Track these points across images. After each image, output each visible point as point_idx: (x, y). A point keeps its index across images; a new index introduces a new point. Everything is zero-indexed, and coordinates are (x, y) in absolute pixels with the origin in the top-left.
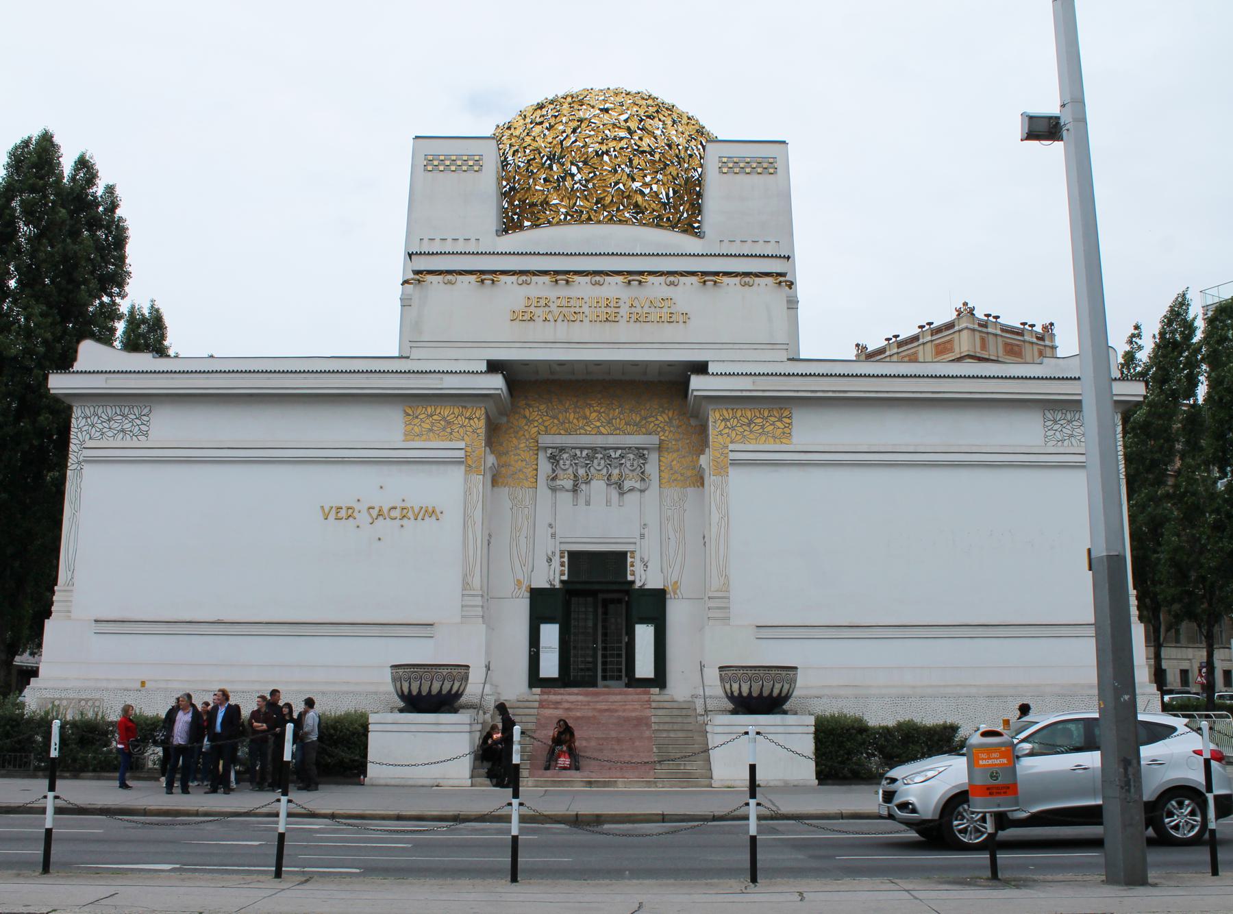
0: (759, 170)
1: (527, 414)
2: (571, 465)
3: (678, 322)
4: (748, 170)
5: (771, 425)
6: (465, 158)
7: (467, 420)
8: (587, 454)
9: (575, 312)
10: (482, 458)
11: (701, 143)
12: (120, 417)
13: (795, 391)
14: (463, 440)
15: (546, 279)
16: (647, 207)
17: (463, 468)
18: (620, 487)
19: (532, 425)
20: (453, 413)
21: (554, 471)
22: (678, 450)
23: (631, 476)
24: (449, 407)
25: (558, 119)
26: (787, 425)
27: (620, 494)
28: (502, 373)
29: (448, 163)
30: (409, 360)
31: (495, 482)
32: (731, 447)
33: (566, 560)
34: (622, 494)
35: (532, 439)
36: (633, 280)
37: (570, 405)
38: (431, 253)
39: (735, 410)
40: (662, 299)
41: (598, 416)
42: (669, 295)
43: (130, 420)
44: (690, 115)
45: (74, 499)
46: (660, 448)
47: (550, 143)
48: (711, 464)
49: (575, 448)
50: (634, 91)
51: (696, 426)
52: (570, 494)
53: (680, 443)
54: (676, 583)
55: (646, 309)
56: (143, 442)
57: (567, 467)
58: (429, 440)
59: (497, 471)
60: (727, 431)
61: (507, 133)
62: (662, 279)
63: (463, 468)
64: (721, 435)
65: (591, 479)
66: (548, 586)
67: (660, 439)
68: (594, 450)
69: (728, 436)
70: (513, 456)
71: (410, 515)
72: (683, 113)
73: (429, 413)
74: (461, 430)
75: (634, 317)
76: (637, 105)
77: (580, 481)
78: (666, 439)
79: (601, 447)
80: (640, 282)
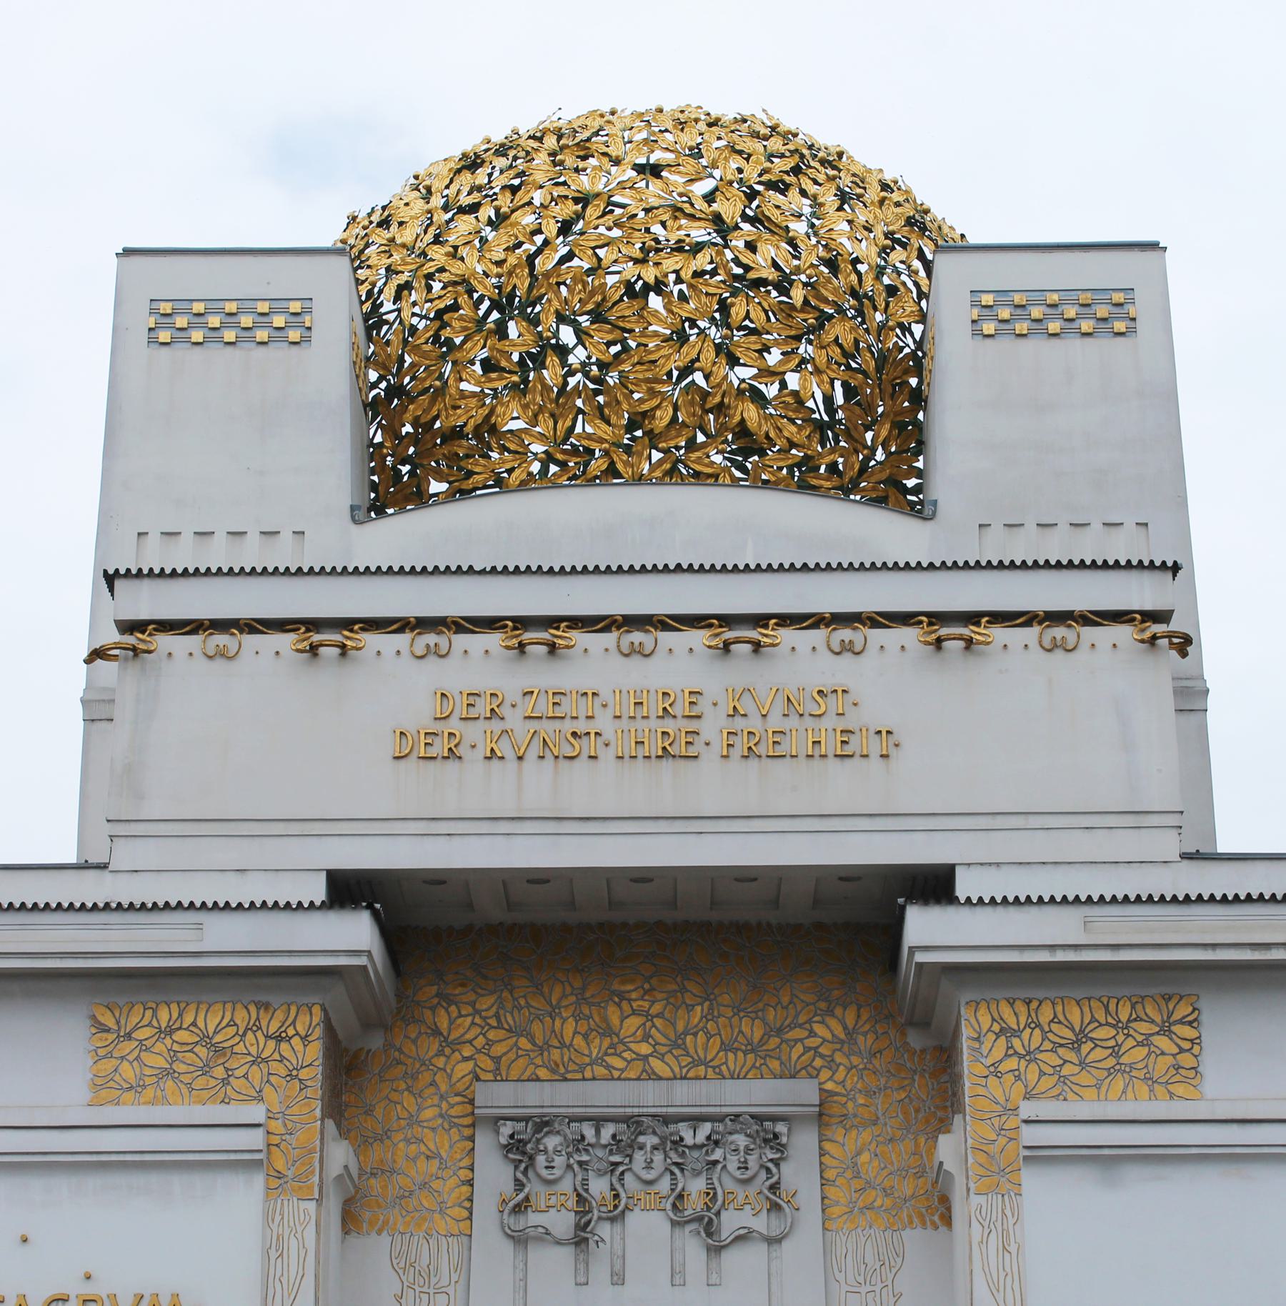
0: (1086, 326)
1: (443, 1024)
2: (569, 1167)
3: (866, 756)
4: (1054, 327)
5: (1140, 1044)
6: (263, 307)
7: (272, 1044)
8: (614, 1136)
9: (574, 734)
10: (312, 1151)
11: (921, 256)
13: (1205, 946)
14: (260, 1099)
15: (494, 640)
16: (772, 435)
17: (259, 1180)
18: (710, 1229)
20: (233, 1023)
21: (519, 1186)
22: (875, 1123)
23: (741, 1199)
24: (220, 1006)
25: (521, 197)
26: (1186, 1045)
27: (709, 1249)
28: (370, 907)
29: (214, 321)
30: (106, 873)
31: (350, 1220)
32: (1028, 1109)
34: (716, 1250)
35: (456, 1095)
36: (738, 641)
37: (564, 996)
38: (168, 571)
39: (1034, 1005)
40: (820, 692)
41: (644, 1024)
44: (888, 177)
46: (822, 1116)
47: (499, 263)
48: (970, 1160)
49: (581, 1119)
50: (728, 112)
51: (923, 1051)
52: (567, 1253)
53: (880, 1102)
55: (775, 722)
57: (557, 1172)
58: (165, 1101)
59: (357, 1189)
60: (1012, 1063)
61: (380, 237)
62: (818, 636)
63: (259, 1180)
64: (998, 1075)
65: (627, 1207)
67: (820, 1089)
68: (634, 1122)
69: (1018, 1078)
70: (401, 1145)
72: (869, 171)
73: (163, 1026)
75: (741, 744)
76: (740, 153)
77: (596, 1212)
78: (839, 1089)
79: (653, 1116)
80: (757, 646)
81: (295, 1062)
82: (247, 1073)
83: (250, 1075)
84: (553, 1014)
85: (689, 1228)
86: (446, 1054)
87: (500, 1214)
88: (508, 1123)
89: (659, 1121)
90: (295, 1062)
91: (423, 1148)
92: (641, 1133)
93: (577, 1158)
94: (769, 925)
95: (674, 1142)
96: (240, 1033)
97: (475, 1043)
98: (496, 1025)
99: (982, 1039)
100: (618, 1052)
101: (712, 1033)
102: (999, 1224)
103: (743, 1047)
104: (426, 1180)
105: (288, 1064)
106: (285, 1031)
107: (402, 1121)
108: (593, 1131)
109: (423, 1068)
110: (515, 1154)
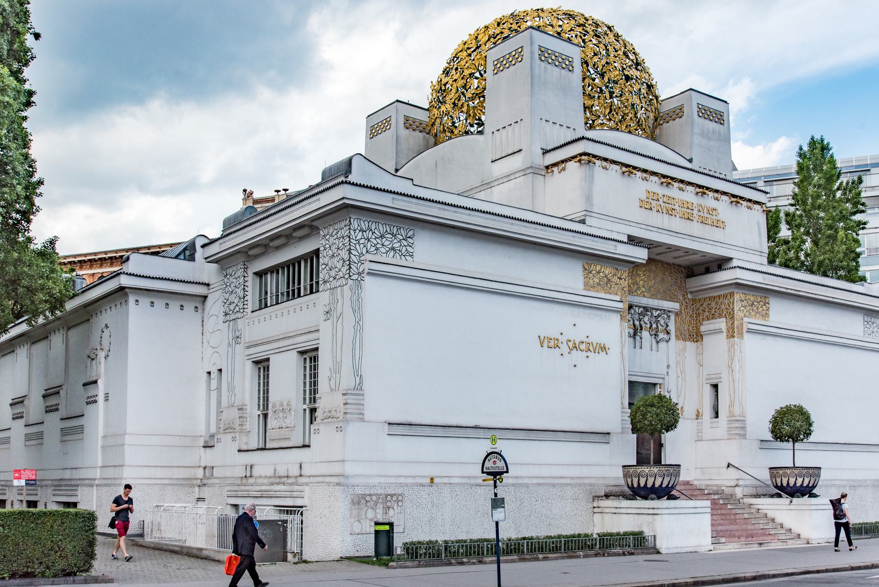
12: (391, 236)
34: (658, 342)
42: (714, 207)
43: (399, 240)
45: (357, 308)
56: (409, 262)
68: (646, 309)
71: (591, 349)
74: (616, 287)
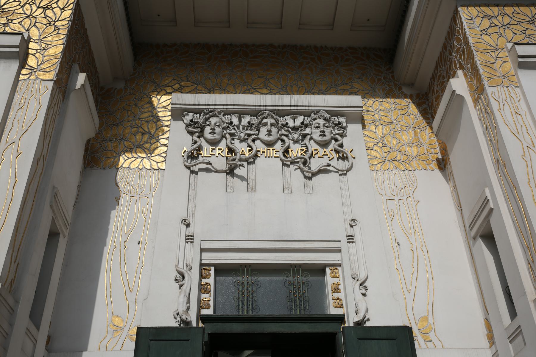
7: (40, 10)
8: (249, 123)
19: (163, 92)
33: (211, 280)
35: (162, 108)
54: (426, 318)
57: (216, 136)
60: (496, 29)
66: (174, 324)
79: (271, 111)
81: (54, 19)
82: (21, 22)
83: (23, 23)
84: (216, 77)
85: (291, 166)
86: (158, 91)
87: (183, 158)
88: (191, 114)
89: (274, 113)
90: (54, 19)
91: (141, 130)
92: (265, 118)
93: (228, 131)
94: (326, 47)
95: (282, 125)
96: (21, 5)
97: (173, 87)
98: (186, 80)
99: (474, 20)
100: (251, 92)
101: (300, 86)
102: (509, 100)
103: (317, 92)
104: (141, 143)
105: (49, 19)
106: (51, 5)
107: (130, 118)
108: (237, 119)
109: (145, 96)
110: (193, 128)
